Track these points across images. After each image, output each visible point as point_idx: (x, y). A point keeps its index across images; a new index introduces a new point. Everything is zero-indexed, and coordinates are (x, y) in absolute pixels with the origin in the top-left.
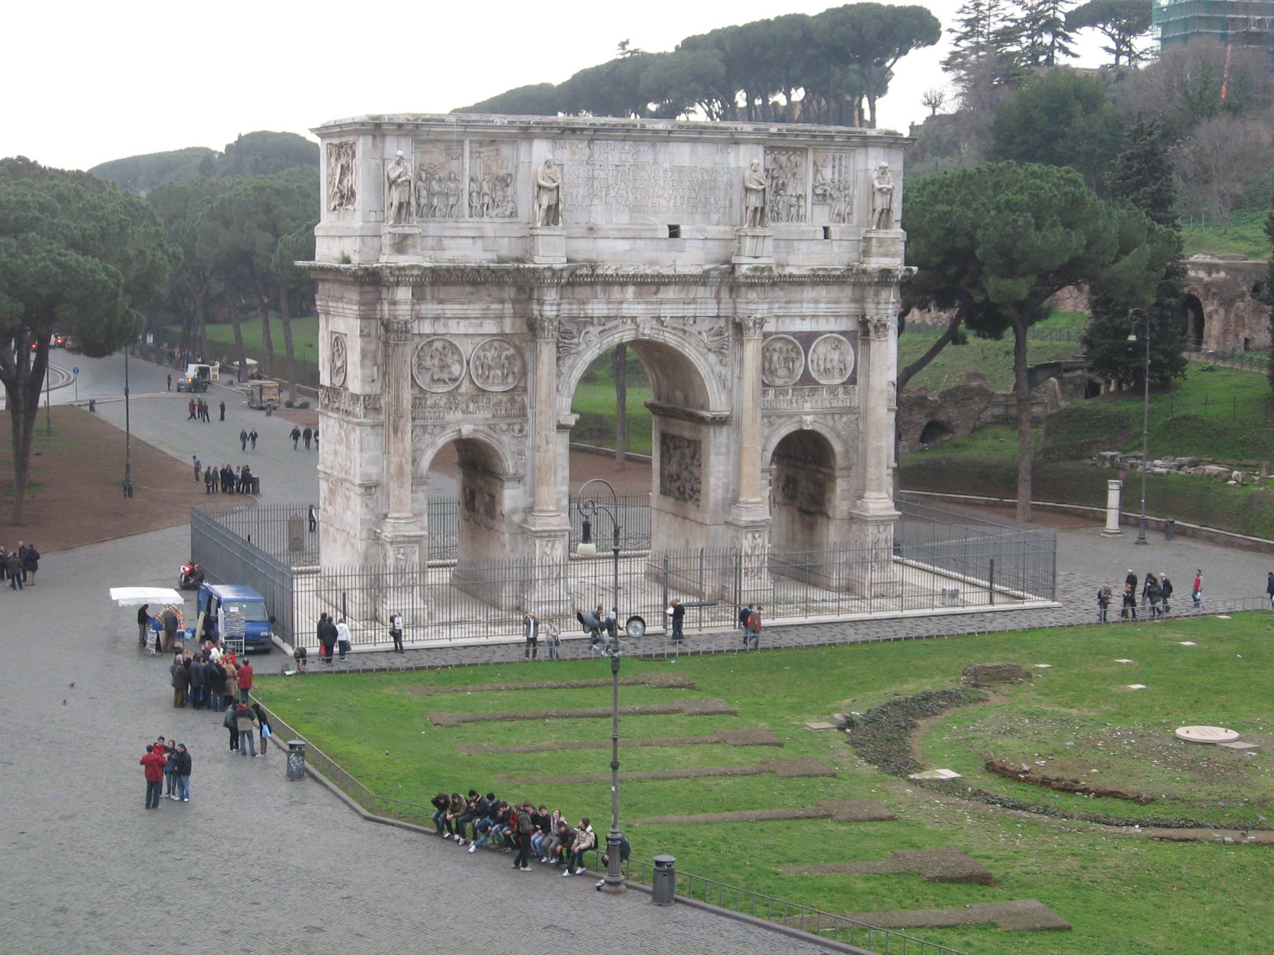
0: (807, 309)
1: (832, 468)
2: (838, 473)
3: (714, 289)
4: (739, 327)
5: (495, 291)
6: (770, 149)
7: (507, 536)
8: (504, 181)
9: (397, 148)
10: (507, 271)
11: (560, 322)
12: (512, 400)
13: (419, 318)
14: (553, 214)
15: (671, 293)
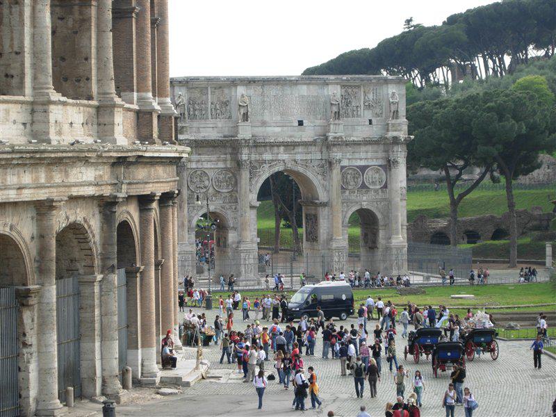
0: (363, 155)
1: (377, 225)
2: (380, 228)
3: (320, 147)
4: (330, 164)
5: (223, 150)
6: (343, 86)
7: (230, 253)
8: (226, 104)
9: (181, 92)
10: (227, 141)
11: (251, 163)
12: (231, 196)
13: (190, 161)
14: (246, 117)
15: (300, 149)
